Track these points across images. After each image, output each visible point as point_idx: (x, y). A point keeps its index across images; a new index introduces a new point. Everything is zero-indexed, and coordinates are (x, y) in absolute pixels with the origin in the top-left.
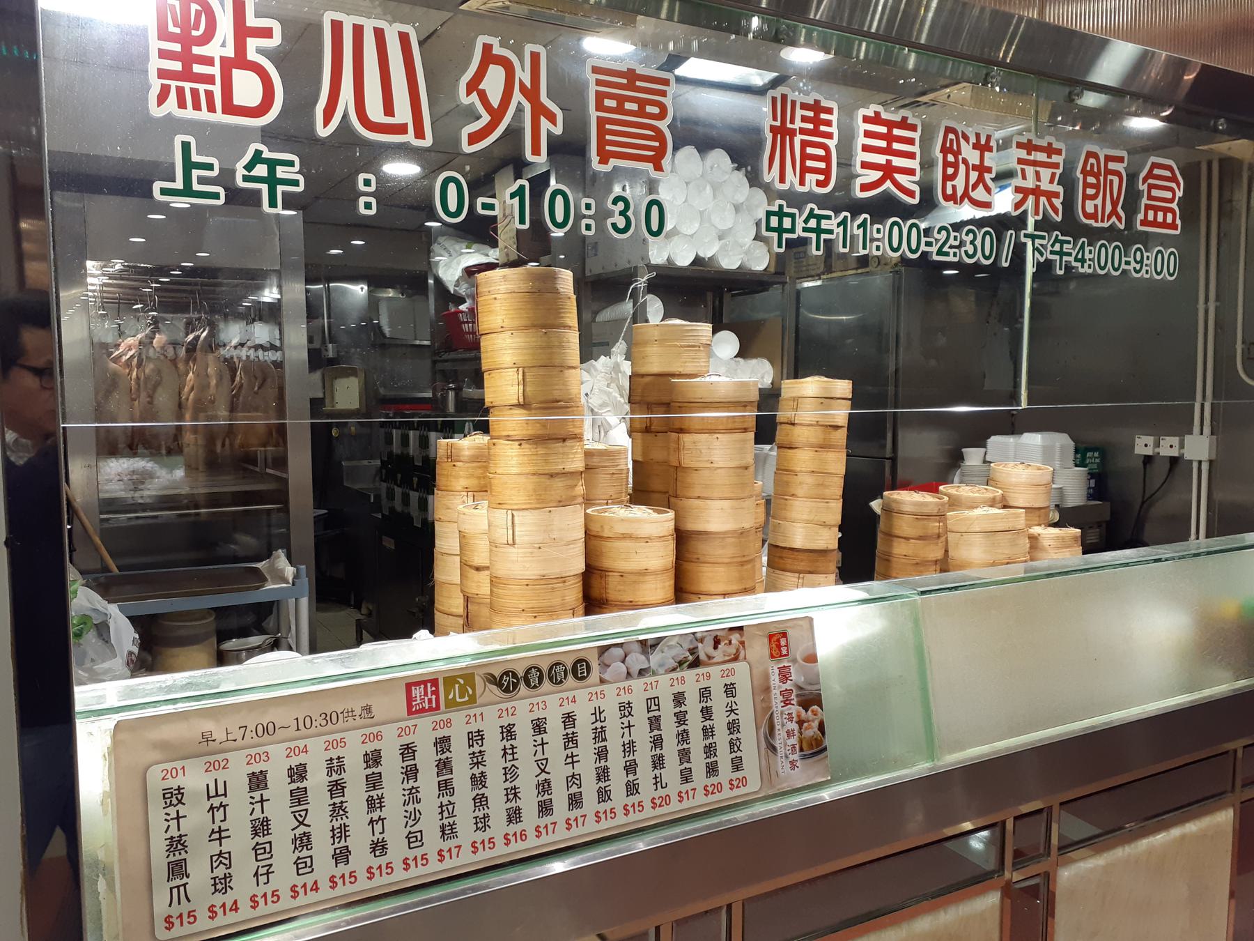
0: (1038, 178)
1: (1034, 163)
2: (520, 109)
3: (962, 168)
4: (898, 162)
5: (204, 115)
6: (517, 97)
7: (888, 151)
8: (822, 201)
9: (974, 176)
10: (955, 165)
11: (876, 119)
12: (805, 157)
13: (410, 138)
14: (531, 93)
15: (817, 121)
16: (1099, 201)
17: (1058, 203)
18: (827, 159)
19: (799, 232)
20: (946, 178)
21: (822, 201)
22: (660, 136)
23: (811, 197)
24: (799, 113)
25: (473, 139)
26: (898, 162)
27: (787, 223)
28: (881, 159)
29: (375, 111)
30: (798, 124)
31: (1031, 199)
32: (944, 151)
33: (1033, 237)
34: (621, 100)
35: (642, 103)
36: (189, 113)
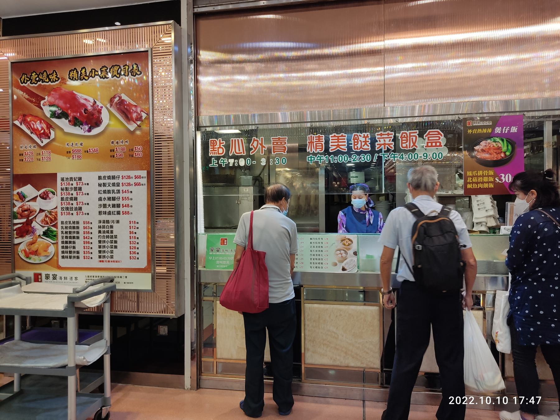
0: (385, 141)
1: (383, 138)
2: (259, 148)
3: (360, 142)
4: (340, 144)
7: (338, 142)
8: (321, 154)
9: (363, 144)
10: (358, 142)
11: (335, 136)
12: (316, 146)
14: (261, 144)
15: (319, 139)
16: (408, 144)
17: (392, 146)
18: (322, 146)
19: (316, 160)
20: (355, 145)
21: (321, 154)
22: (285, 147)
23: (318, 153)
24: (315, 138)
26: (340, 144)
27: (313, 159)
28: (336, 144)
29: (237, 151)
30: (315, 140)
31: (383, 146)
32: (354, 139)
33: (384, 155)
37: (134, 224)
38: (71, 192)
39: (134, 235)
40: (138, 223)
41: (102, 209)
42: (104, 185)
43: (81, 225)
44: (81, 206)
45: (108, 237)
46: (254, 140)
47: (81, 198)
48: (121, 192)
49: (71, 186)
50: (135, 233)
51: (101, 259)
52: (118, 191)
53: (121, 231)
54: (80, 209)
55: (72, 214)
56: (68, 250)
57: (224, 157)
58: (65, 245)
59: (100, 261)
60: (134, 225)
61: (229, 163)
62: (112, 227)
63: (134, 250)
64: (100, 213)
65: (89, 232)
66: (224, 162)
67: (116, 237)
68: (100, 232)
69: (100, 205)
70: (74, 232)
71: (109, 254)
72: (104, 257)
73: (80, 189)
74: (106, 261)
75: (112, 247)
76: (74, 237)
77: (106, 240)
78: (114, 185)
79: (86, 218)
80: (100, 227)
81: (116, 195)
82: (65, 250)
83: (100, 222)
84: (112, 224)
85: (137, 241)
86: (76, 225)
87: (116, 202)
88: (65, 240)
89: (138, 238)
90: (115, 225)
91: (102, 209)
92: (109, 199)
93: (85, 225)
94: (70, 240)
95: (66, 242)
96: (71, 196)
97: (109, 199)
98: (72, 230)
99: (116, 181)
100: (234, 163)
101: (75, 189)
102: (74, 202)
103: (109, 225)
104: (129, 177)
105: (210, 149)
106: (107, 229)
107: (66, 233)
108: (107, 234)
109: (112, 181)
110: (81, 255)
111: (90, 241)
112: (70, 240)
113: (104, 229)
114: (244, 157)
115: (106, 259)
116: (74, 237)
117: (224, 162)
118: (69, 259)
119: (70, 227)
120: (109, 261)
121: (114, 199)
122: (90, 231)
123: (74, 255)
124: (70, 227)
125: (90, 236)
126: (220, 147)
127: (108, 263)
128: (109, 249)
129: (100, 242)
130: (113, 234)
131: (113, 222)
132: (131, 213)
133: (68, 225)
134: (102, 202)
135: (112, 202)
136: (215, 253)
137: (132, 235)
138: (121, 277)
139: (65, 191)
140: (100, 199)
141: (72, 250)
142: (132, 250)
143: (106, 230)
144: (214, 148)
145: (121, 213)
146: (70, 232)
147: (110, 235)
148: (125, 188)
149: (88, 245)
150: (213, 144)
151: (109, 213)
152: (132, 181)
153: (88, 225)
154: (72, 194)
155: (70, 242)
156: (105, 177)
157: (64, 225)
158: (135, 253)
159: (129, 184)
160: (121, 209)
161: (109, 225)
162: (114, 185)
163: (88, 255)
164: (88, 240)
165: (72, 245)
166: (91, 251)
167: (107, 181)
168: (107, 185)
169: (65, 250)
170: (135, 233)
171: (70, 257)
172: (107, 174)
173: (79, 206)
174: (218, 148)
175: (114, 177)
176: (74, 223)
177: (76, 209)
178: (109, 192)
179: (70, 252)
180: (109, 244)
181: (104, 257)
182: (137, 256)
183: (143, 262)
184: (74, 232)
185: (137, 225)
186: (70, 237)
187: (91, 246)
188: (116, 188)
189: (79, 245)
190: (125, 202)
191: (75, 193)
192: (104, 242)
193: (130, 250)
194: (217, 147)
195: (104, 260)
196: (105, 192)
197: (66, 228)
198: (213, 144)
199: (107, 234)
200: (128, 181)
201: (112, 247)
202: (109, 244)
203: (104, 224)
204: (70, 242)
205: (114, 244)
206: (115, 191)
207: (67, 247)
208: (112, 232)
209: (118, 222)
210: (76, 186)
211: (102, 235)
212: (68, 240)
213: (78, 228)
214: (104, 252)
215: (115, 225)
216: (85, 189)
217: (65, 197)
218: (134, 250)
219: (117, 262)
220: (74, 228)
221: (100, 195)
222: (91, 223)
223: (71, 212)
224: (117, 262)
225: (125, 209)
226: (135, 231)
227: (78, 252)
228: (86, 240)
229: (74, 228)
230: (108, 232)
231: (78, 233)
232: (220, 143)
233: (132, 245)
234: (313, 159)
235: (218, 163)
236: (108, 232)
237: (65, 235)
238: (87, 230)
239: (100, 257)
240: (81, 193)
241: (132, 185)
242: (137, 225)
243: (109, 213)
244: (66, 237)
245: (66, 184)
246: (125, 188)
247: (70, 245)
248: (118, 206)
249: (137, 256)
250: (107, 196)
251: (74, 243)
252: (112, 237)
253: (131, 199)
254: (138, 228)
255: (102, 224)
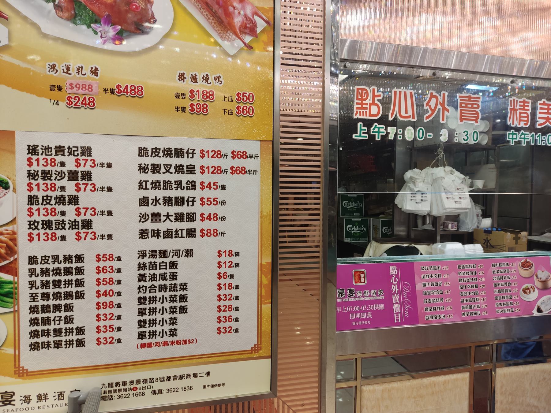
2: (439, 109)
5: (365, 117)
6: (439, 106)
13: (411, 119)
22: (477, 113)
25: (427, 118)
34: (467, 104)
35: (473, 104)
36: (362, 117)
37: (229, 258)
38: (59, 184)
39: (228, 281)
40: (237, 254)
41: (149, 225)
42: (155, 169)
43: (90, 265)
44: (88, 217)
45: (163, 288)
46: (432, 96)
47: (87, 199)
48: (198, 186)
49: (59, 169)
50: (232, 276)
51: (146, 341)
52: (192, 185)
53: (197, 274)
54: (88, 224)
55: (63, 238)
56: (52, 327)
57: (379, 121)
58: (40, 316)
59: (143, 346)
60: (228, 259)
61: (388, 134)
62: (173, 265)
63: (227, 314)
64: (143, 234)
65: (111, 280)
66: (379, 132)
67: (184, 287)
68: (142, 278)
69: (144, 217)
70: (69, 283)
71: (167, 328)
72: (153, 334)
73: (87, 176)
74: (158, 344)
75: (173, 310)
76: (68, 295)
77: (159, 295)
78: (179, 169)
79: (104, 247)
80: (142, 266)
81: (186, 194)
82: (40, 328)
83: (143, 254)
84: (175, 258)
85: (234, 292)
86: (74, 265)
87: (184, 209)
88: (41, 303)
89: (237, 287)
90: (182, 261)
91: (149, 225)
92: (168, 201)
93: (101, 264)
94: (57, 302)
95: (45, 309)
96: (59, 193)
97: (168, 201)
98: (63, 278)
99: (185, 161)
100: (396, 135)
101: (73, 176)
102: (70, 210)
103: (167, 260)
104: (218, 154)
105: (356, 106)
106: (162, 271)
107: (45, 284)
108: (162, 282)
109: (174, 161)
110: (90, 336)
111: (116, 300)
112: (57, 302)
113: (152, 272)
114: (414, 125)
115: (158, 339)
116: (68, 295)
117: (379, 132)
118: (53, 351)
119: (57, 271)
120: (165, 344)
121: (180, 201)
122: (116, 276)
123: (70, 338)
124: (57, 271)
125: (116, 288)
126: (373, 103)
127: (162, 348)
128: (167, 316)
129: (142, 301)
130: (178, 282)
131: (177, 253)
132: (223, 234)
133: (51, 266)
134: (150, 209)
135: (173, 210)
136: (346, 300)
137: (223, 281)
138: (195, 375)
139: (40, 181)
140: (144, 202)
141: (63, 326)
142: (222, 314)
143: (158, 272)
144: (362, 104)
145: (198, 233)
146: (57, 284)
147: (168, 283)
148: (207, 178)
149: (108, 311)
150: (362, 96)
151: (168, 234)
152: (226, 163)
153: (108, 264)
154: (63, 189)
155: (57, 308)
156: (156, 152)
157: (38, 268)
158: (230, 319)
159: (219, 170)
160: (197, 225)
161: (167, 260)
162: (179, 169)
163: (108, 335)
164: (108, 299)
165: (63, 314)
166: (116, 323)
167: (162, 161)
168: (163, 170)
169: (40, 328)
170: (232, 276)
171: (58, 345)
172: (162, 144)
173: (82, 217)
174: (371, 104)
175: (180, 153)
176: (68, 259)
177: (74, 225)
178: (167, 185)
179: (58, 332)
180: (167, 305)
181: (153, 334)
182: (234, 325)
183: (248, 336)
184: (69, 283)
185: (235, 260)
186: (57, 296)
187: (116, 312)
188: (185, 178)
189: (84, 313)
190: (208, 210)
191: (70, 188)
192: (154, 300)
193: (218, 314)
194: (367, 101)
195: (153, 341)
196: (156, 185)
197: (45, 272)
198: (362, 96)
199: (162, 282)
200: (216, 162)
201: (173, 310)
202: (167, 305)
203: (152, 260)
204: (57, 308)
205: (178, 304)
206: (184, 184)
207: (46, 321)
208: (174, 276)
209: (189, 253)
210: (74, 168)
211: (148, 284)
212: (51, 302)
213: (80, 271)
214: (154, 322)
215: (182, 261)
216: (100, 177)
217: (40, 194)
218: (227, 314)
219: (185, 342)
220: (68, 271)
221: (143, 193)
222: (119, 259)
223: (59, 233)
224: (185, 342)
225: (208, 225)
226: (229, 271)
227: (80, 331)
228: (102, 299)
229: (68, 271)
230: (163, 277)
231: (80, 283)
232: (374, 96)
233: (222, 303)
234: (515, 136)
235: (368, 133)
236: (163, 277)
237: (40, 291)
238: (108, 276)
239: (142, 336)
240: (90, 187)
241: (226, 171)
242: (235, 260)
243: (168, 234)
244: (45, 296)
245: (42, 162)
246: (207, 178)
247: (58, 314)
248: (191, 217)
249: (234, 325)
250: (161, 194)
251: (69, 308)
252: (173, 288)
253: (223, 203)
254: (237, 265)
255: (147, 260)
